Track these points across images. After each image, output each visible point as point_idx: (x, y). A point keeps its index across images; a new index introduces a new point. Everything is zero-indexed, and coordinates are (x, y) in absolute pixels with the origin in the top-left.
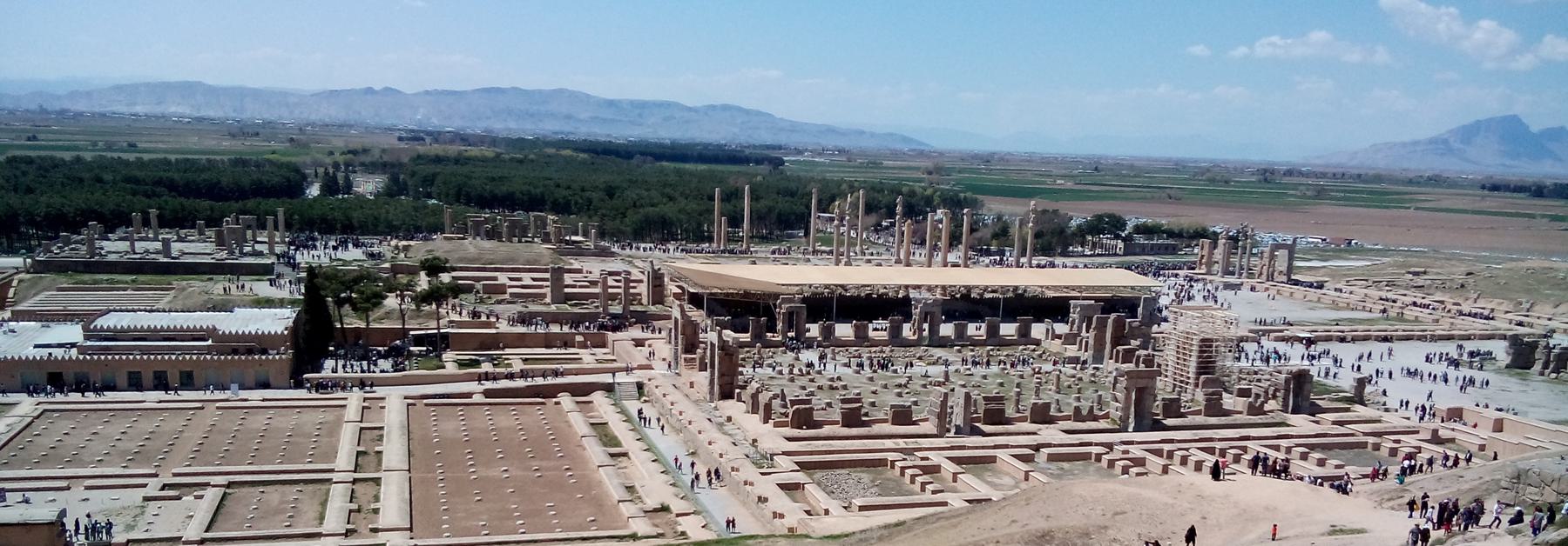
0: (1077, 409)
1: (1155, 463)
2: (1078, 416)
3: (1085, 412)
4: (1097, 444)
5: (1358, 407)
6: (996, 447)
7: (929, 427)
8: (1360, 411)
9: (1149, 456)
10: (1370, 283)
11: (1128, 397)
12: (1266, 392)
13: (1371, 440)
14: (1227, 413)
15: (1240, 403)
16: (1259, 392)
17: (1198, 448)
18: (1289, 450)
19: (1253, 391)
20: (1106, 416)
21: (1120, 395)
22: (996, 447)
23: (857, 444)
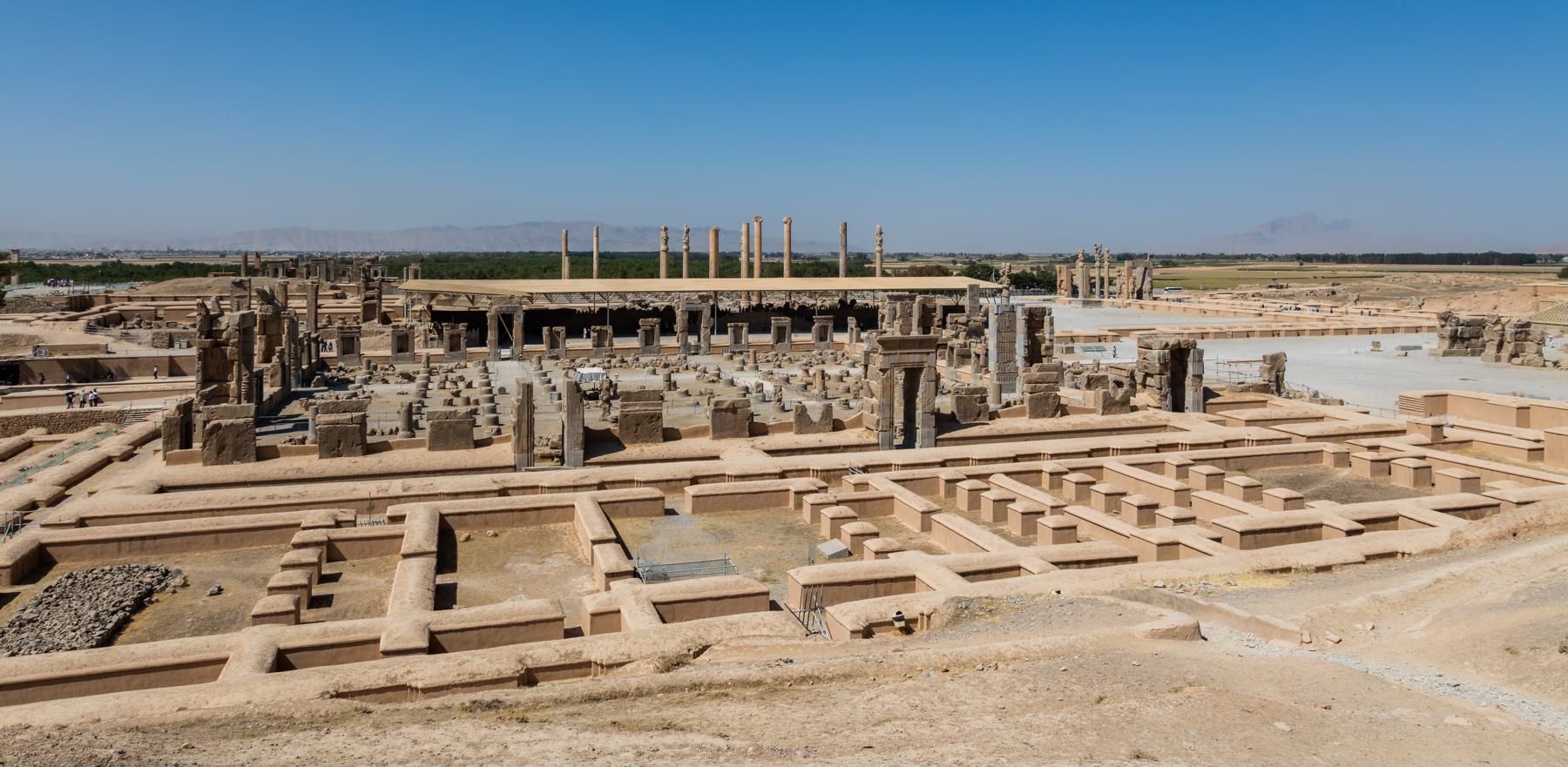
0: (802, 413)
1: (911, 503)
2: (803, 421)
3: (815, 416)
4: (647, 483)
5: (1275, 400)
6: (575, 488)
7: (504, 451)
8: (1278, 406)
9: (899, 492)
10: (1235, 296)
11: (888, 388)
12: (1132, 376)
13: (1330, 447)
14: (1063, 410)
15: (1091, 397)
16: (1118, 379)
17: (1007, 474)
18: (1182, 471)
19: (1109, 379)
20: (857, 423)
21: (875, 385)
22: (575, 488)
23: (261, 494)
